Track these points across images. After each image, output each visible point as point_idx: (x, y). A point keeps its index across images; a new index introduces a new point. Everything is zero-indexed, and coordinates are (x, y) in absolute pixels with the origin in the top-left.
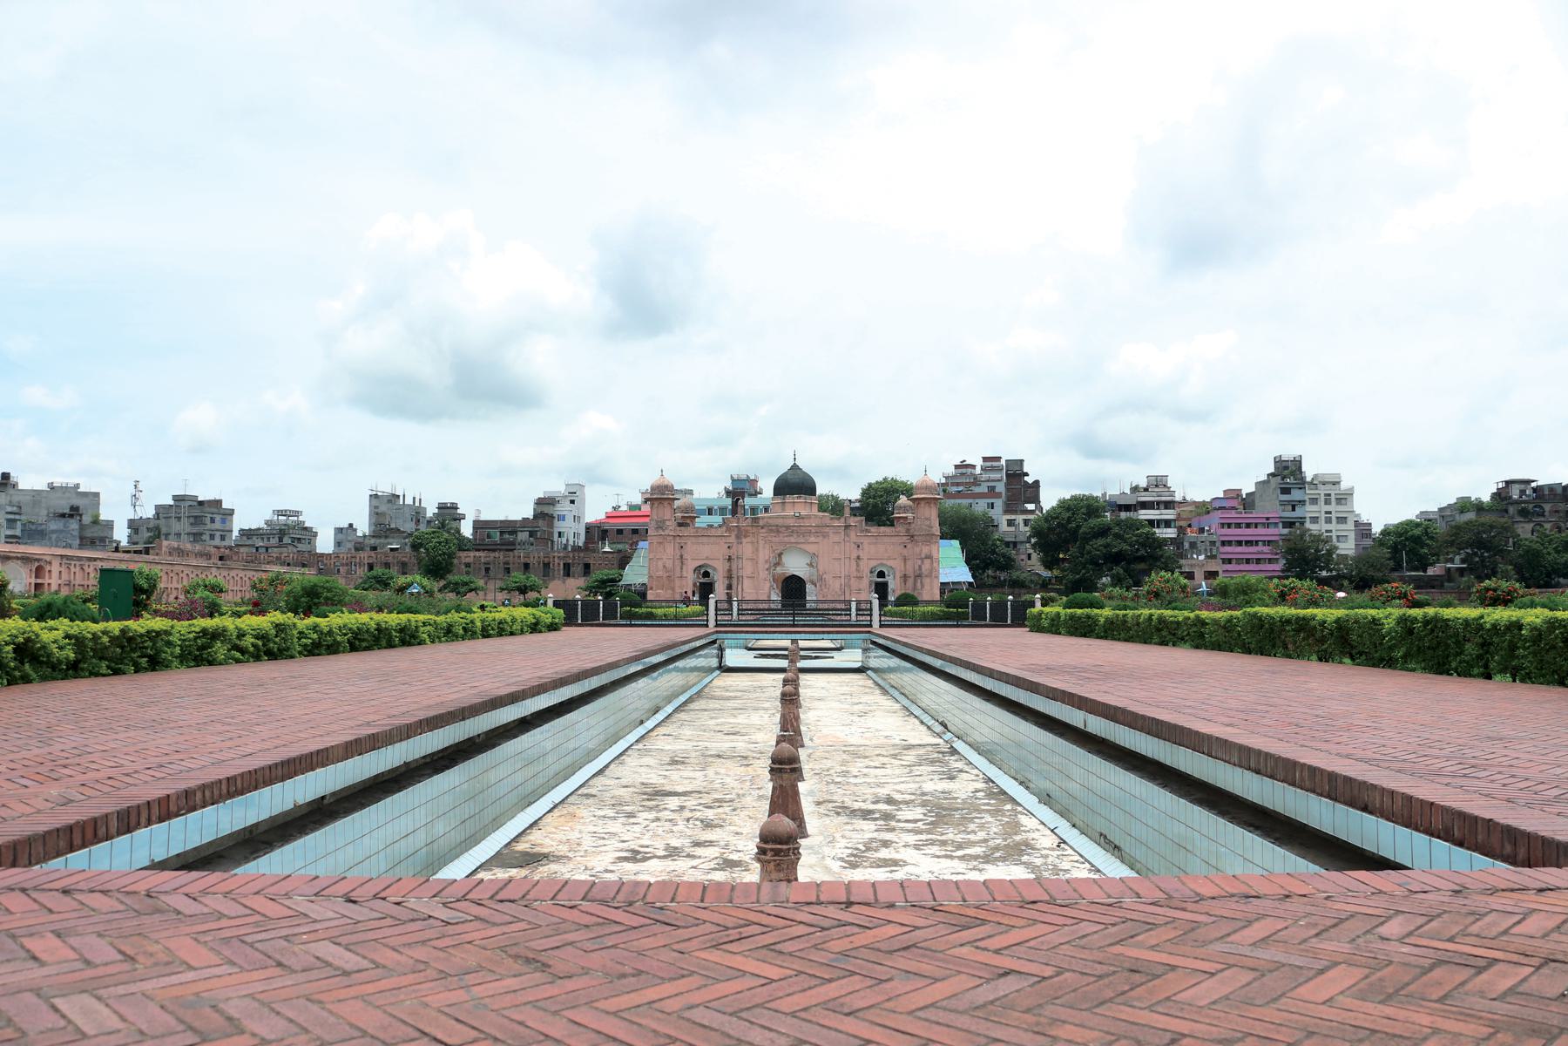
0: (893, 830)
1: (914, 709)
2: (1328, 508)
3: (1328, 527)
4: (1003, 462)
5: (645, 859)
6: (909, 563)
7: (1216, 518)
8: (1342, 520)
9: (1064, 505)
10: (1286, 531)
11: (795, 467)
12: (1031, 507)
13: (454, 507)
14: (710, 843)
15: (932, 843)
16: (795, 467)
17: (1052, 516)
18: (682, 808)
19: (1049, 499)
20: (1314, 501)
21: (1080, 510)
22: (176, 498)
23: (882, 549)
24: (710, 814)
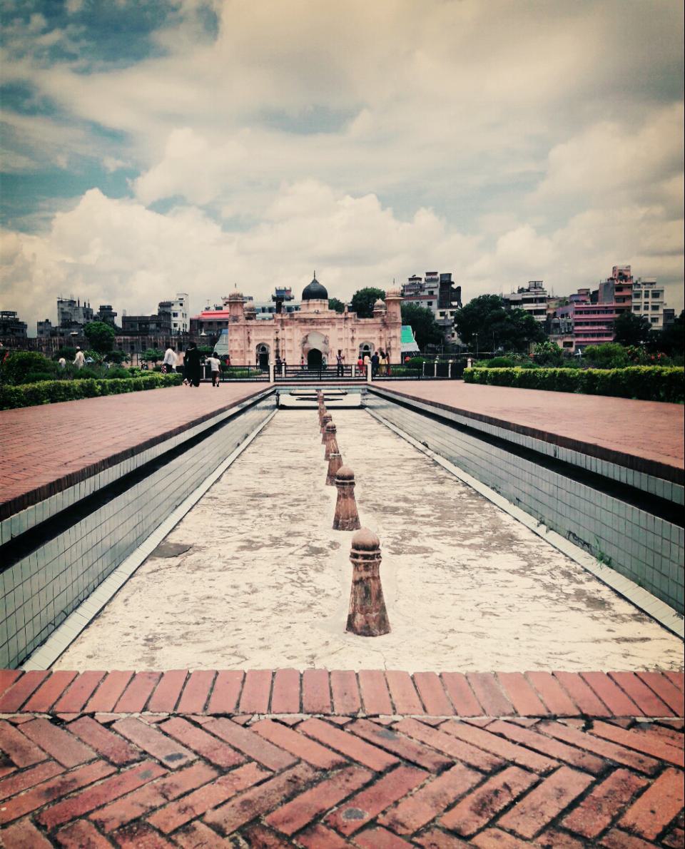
0: (416, 522)
1: (401, 433)
2: (647, 300)
3: (646, 312)
4: (438, 276)
5: (258, 548)
7: (570, 309)
9: (474, 301)
10: (617, 316)
12: (455, 303)
14: (299, 534)
15: (446, 534)
17: (469, 308)
18: (275, 506)
19: (466, 300)
20: (638, 296)
21: (487, 304)
23: (369, 333)
24: (293, 510)
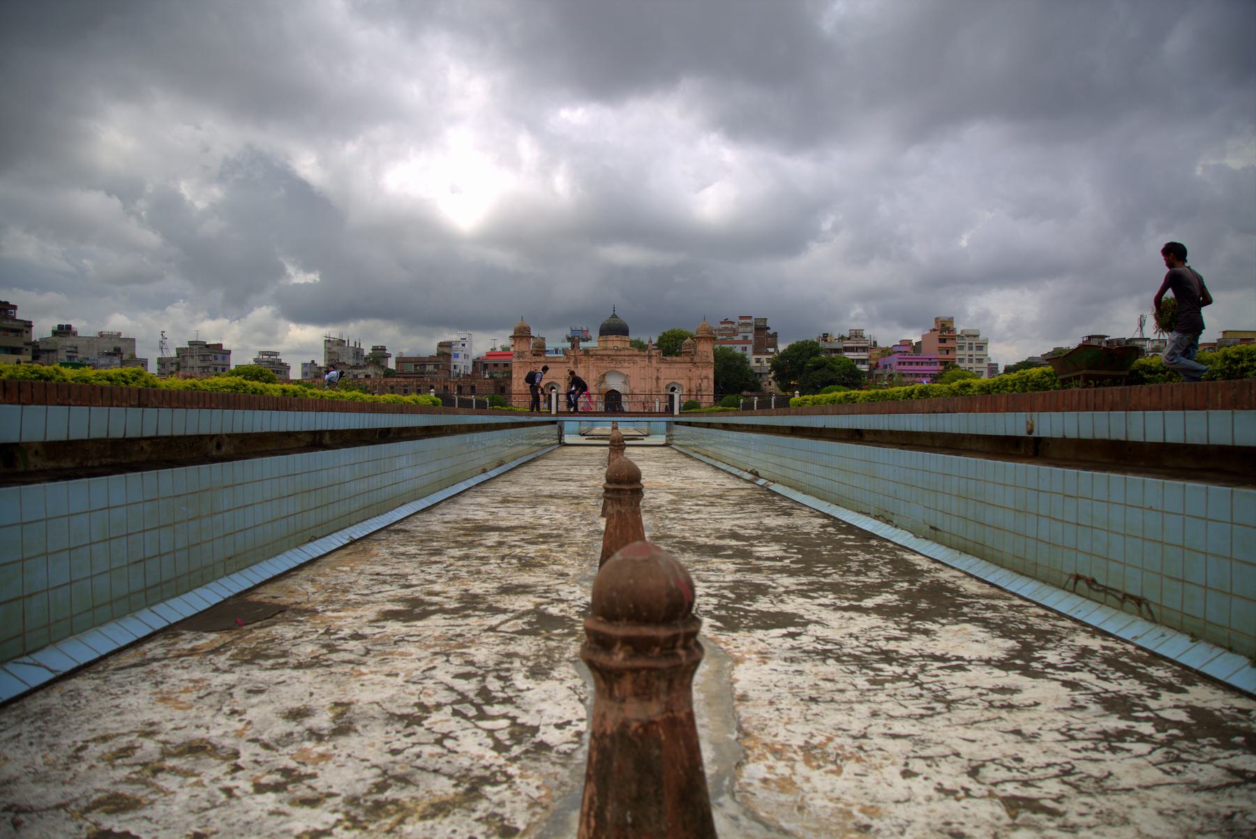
0: (758, 570)
1: (718, 464)
5: (425, 615)
6: (693, 383)
7: (894, 360)
8: (980, 361)
11: (614, 316)
12: (771, 350)
13: (383, 349)
14: (524, 589)
15: (821, 588)
16: (614, 316)
17: (783, 356)
18: (500, 544)
20: (961, 348)
22: (191, 343)
24: (532, 550)
